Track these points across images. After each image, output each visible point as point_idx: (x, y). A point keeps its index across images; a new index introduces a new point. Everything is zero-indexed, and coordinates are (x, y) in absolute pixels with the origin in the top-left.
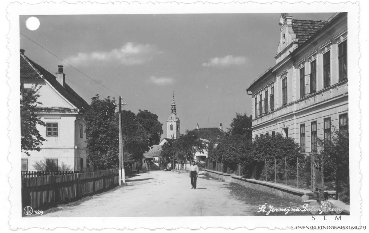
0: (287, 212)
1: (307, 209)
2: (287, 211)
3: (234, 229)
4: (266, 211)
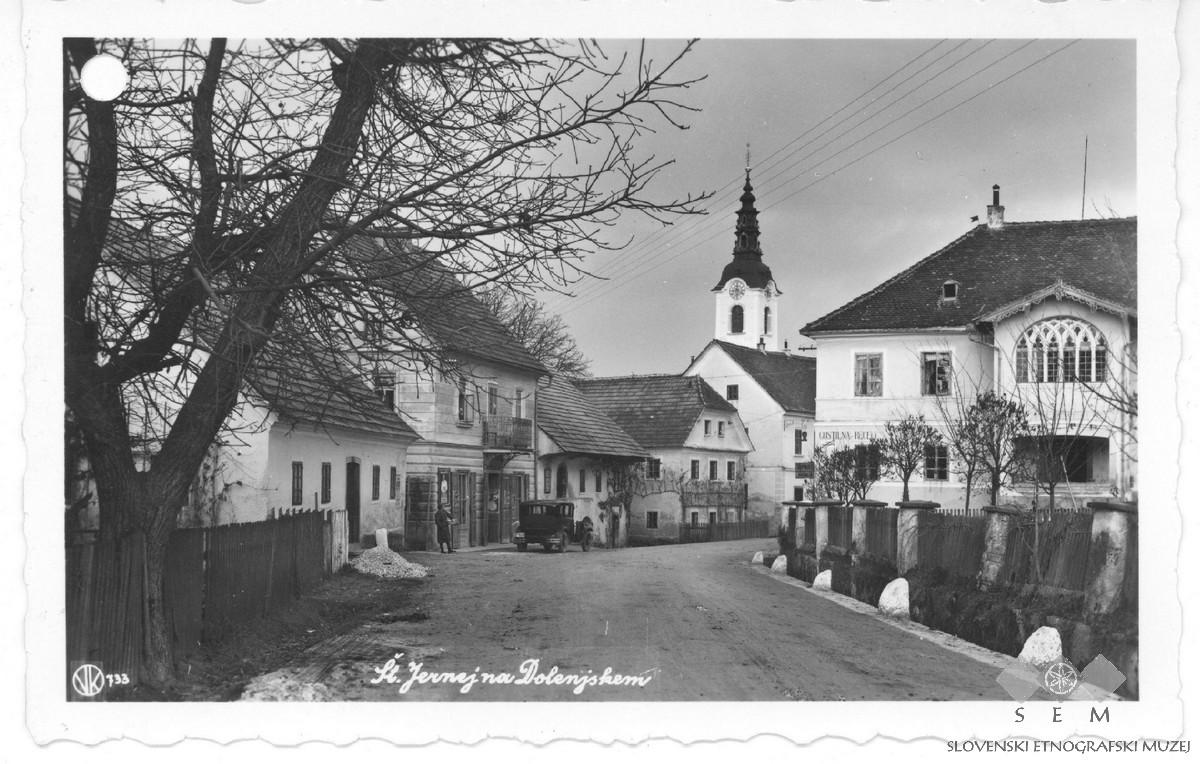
0: (469, 686)
1: (536, 676)
2: (469, 681)
3: (636, 741)
4: (399, 681)
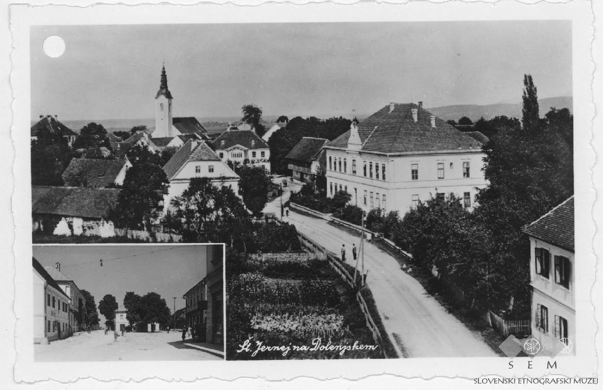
2: (286, 350)
